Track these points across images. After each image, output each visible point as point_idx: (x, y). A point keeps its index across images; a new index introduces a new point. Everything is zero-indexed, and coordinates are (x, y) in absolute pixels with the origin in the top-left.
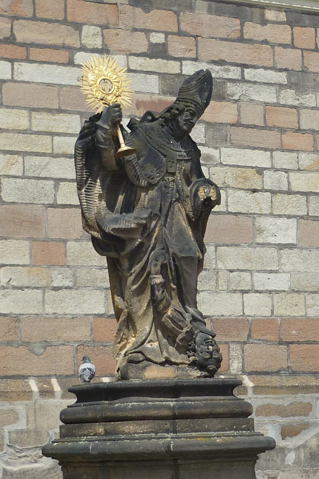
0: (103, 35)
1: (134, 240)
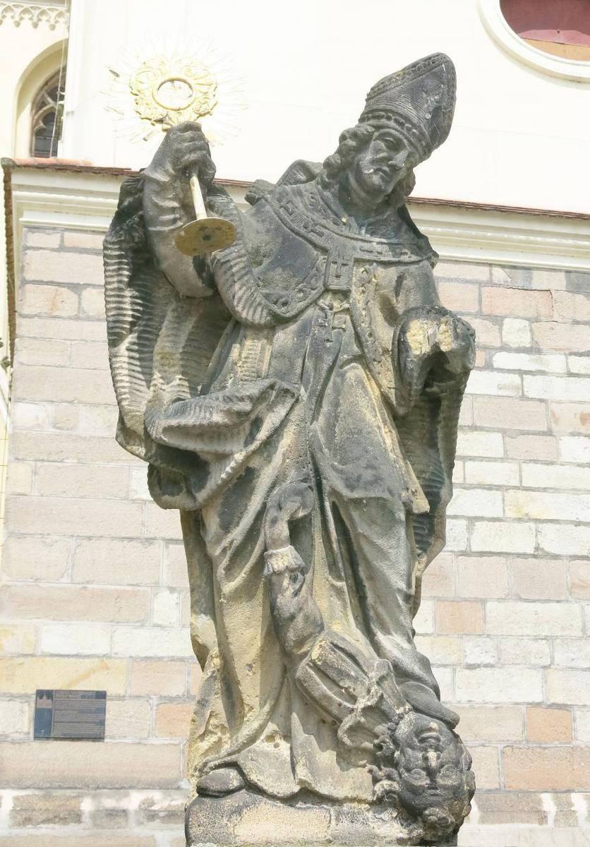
0: (531, 330)
1: (223, 457)
